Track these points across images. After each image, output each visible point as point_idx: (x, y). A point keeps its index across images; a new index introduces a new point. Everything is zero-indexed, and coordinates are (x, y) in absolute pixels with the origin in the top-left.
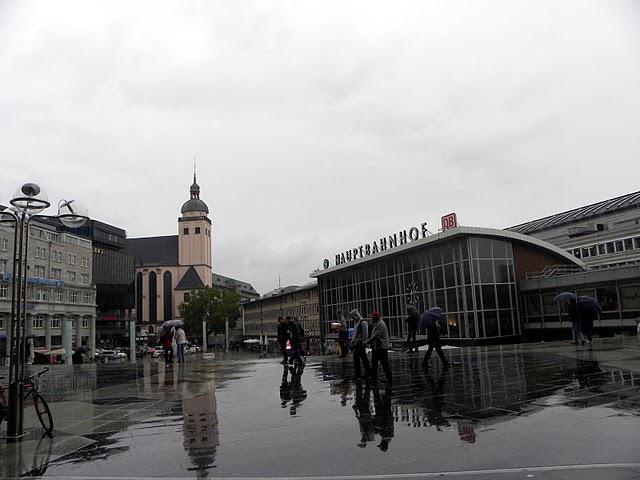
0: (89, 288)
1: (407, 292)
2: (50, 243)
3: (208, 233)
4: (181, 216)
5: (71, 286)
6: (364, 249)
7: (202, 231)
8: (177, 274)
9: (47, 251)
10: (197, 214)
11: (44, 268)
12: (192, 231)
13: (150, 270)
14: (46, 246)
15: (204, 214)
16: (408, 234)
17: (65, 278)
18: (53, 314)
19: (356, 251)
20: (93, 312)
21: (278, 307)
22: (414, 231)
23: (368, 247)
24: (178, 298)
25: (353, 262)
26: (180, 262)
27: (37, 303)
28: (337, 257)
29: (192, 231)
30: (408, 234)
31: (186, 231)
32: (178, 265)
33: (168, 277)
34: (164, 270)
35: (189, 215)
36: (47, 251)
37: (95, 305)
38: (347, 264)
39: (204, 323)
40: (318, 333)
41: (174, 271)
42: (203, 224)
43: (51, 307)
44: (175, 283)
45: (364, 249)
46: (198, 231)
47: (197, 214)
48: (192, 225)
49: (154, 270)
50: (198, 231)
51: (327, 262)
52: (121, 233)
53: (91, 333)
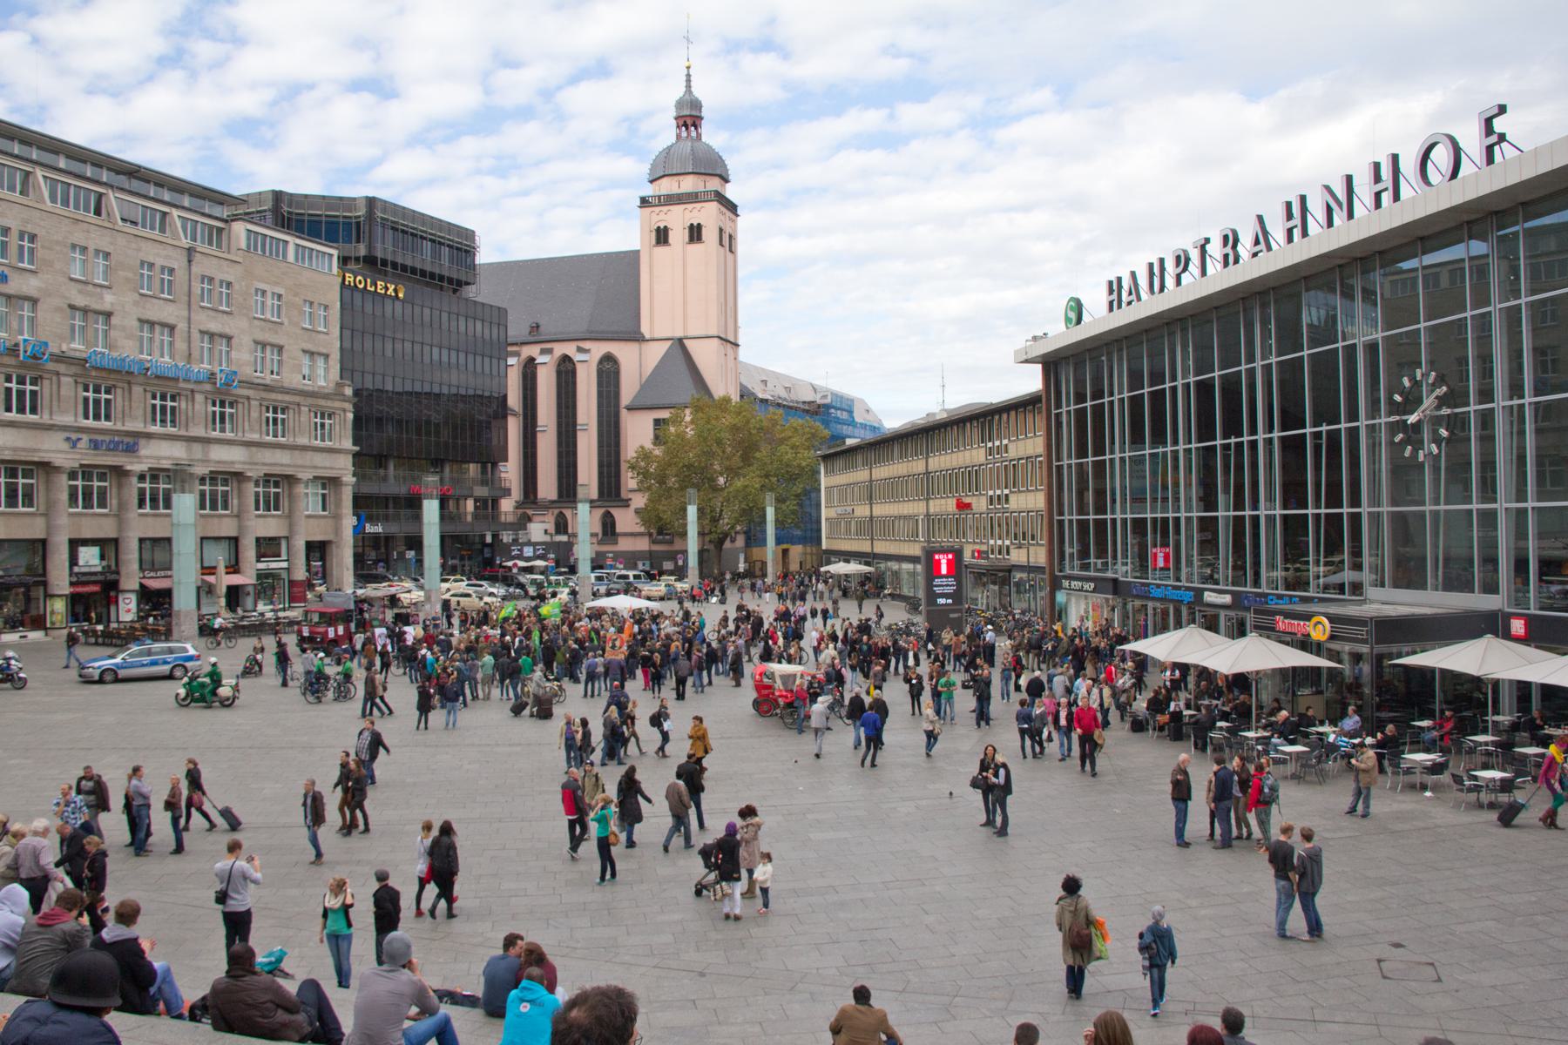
0: (326, 397)
1: (1394, 408)
2: (190, 251)
3: (728, 241)
4: (649, 191)
5: (267, 388)
6: (1215, 249)
7: (710, 234)
8: (637, 364)
9: (181, 274)
10: (688, 184)
11: (172, 328)
12: (678, 235)
13: (560, 349)
14: (178, 262)
15: (714, 184)
16: (1409, 166)
17: (243, 359)
18: (201, 470)
19: (1182, 261)
20: (344, 467)
21: (918, 466)
22: (1441, 156)
23: (1230, 240)
24: (638, 433)
25: (1174, 297)
26: (645, 330)
27: (149, 436)
28: (1114, 287)
29: (678, 235)
30: (1409, 166)
31: (662, 236)
32: (636, 337)
33: (609, 371)
34: (598, 350)
35: (668, 186)
36: (181, 274)
37: (348, 444)
38: (1149, 305)
39: (692, 511)
40: (1039, 556)
41: (625, 353)
42: (707, 215)
43: (197, 449)
44: (628, 392)
45: (1215, 249)
46: (695, 233)
47: (688, 184)
48: (677, 219)
49: (569, 349)
50: (695, 233)
51: (1077, 308)
52: (460, 244)
53: (337, 530)
